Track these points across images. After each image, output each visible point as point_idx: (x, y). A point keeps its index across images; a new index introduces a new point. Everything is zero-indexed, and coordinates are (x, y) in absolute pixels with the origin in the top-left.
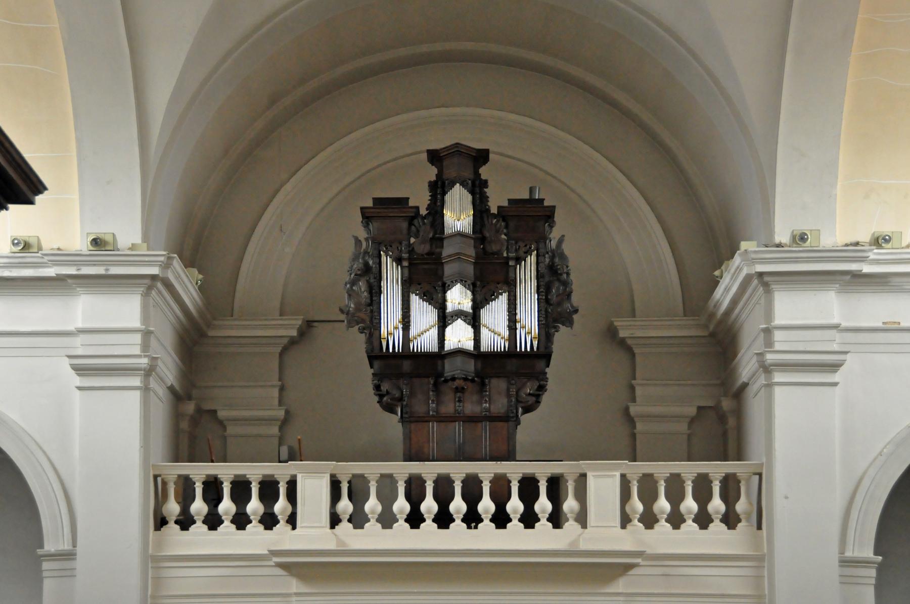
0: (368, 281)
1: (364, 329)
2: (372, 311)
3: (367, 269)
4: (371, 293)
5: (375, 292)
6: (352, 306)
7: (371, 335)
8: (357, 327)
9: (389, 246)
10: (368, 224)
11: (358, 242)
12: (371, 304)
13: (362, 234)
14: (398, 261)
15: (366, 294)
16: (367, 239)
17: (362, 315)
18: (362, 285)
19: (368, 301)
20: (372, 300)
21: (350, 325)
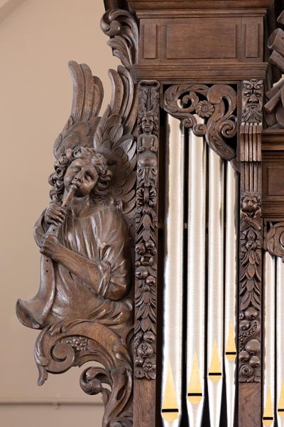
0: (120, 216)
1: (101, 376)
2: (131, 318)
3: (114, 179)
4: (128, 254)
5: (143, 252)
6: (63, 297)
7: (125, 400)
8: (76, 372)
9: (194, 96)
10: (124, 25)
11: (86, 81)
12: (128, 293)
13: (103, 60)
14: (228, 144)
15: (110, 256)
16: (119, 75)
17: (96, 330)
18: (101, 228)
19: (121, 281)
20: (130, 278)
21: (51, 364)
